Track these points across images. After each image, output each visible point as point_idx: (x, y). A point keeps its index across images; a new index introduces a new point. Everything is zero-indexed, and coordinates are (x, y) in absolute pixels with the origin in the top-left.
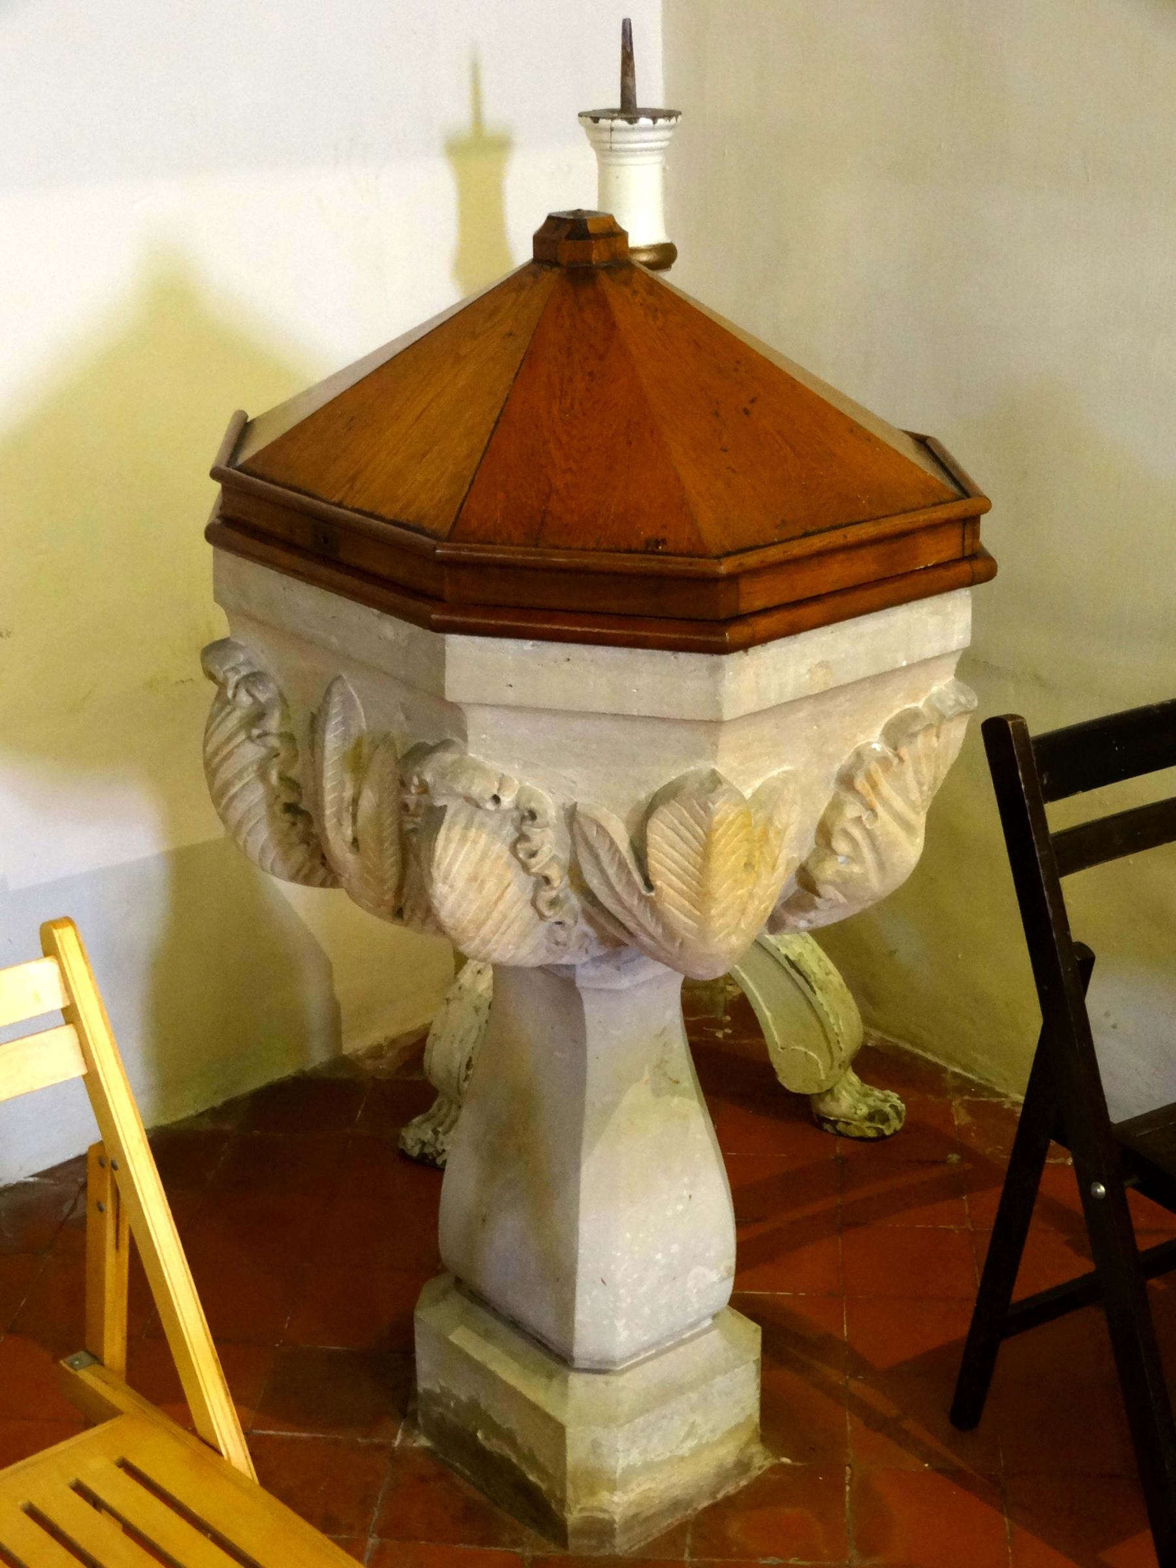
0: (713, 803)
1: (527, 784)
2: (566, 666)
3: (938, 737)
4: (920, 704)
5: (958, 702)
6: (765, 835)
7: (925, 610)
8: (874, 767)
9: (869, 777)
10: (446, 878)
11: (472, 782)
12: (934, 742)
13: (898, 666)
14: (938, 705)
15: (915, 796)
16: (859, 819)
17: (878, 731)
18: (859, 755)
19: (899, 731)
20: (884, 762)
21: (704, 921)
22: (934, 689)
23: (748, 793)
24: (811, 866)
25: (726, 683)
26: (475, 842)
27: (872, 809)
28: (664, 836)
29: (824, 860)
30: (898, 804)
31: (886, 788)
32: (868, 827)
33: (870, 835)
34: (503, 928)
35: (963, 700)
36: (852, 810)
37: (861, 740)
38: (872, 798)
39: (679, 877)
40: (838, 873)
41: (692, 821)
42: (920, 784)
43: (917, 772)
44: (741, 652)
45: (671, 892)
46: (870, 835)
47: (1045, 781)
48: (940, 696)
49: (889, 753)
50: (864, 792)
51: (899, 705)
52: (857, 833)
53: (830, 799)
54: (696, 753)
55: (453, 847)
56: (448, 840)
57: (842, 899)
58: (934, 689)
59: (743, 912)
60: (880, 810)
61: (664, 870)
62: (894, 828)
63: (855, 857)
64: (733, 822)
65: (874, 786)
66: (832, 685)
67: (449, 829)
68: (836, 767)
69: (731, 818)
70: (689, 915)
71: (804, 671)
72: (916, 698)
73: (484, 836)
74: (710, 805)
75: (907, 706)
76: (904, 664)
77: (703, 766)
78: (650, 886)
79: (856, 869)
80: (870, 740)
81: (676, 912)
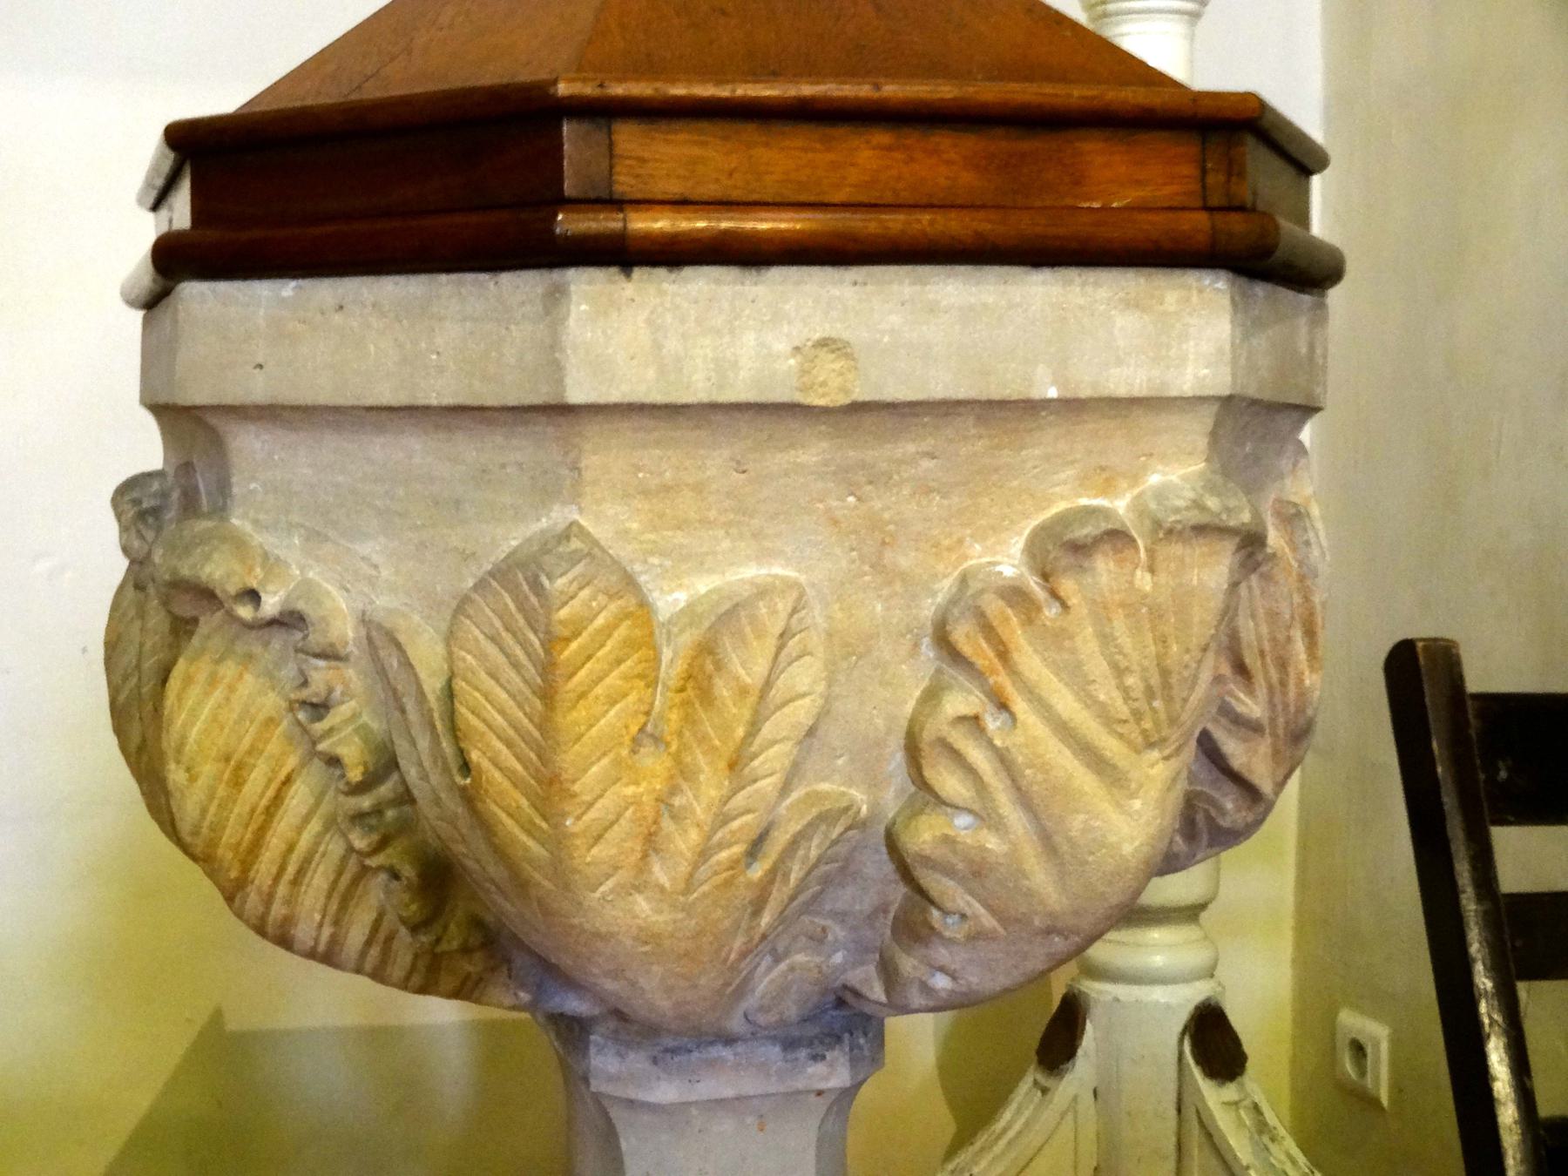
0: (550, 578)
1: (311, 575)
2: (338, 318)
3: (1152, 570)
4: (1121, 505)
5: (1197, 505)
6: (699, 683)
7: (1103, 293)
8: (994, 607)
9: (988, 629)
10: (179, 750)
11: (207, 558)
12: (1144, 581)
13: (1036, 394)
14: (1153, 506)
15: (1106, 692)
16: (973, 722)
17: (1017, 545)
18: (964, 580)
19: (1066, 548)
20: (1015, 595)
21: (557, 841)
22: (1154, 479)
23: (669, 600)
24: (898, 827)
25: (571, 321)
26: (231, 689)
27: (1003, 706)
28: (482, 657)
29: (921, 812)
30: (1066, 703)
31: (1030, 661)
32: (998, 742)
33: (1003, 759)
34: (291, 870)
35: (1212, 503)
36: (958, 702)
37: (977, 555)
38: (1002, 679)
39: (509, 744)
40: (947, 840)
41: (522, 622)
42: (1119, 672)
43: (1105, 638)
44: (614, 270)
45: (497, 775)
46: (1003, 759)
47: (1503, 774)
48: (1161, 494)
49: (1034, 584)
50: (980, 663)
51: (1065, 496)
52: (977, 755)
53: (925, 683)
54: (546, 492)
55: (194, 692)
56: (188, 680)
57: (988, 921)
58: (1154, 479)
59: (651, 842)
60: (1020, 706)
61: (482, 727)
62: (1066, 762)
63: (987, 817)
64: (608, 631)
65: (1004, 654)
66: (861, 394)
67: (192, 661)
68: (928, 609)
69: (600, 621)
70: (530, 829)
71: (781, 346)
72: (1108, 488)
73: (248, 678)
74: (546, 582)
75: (1084, 501)
76: (1053, 393)
77: (558, 516)
78: (466, 767)
79: (992, 843)
80: (998, 558)
81: (508, 822)
